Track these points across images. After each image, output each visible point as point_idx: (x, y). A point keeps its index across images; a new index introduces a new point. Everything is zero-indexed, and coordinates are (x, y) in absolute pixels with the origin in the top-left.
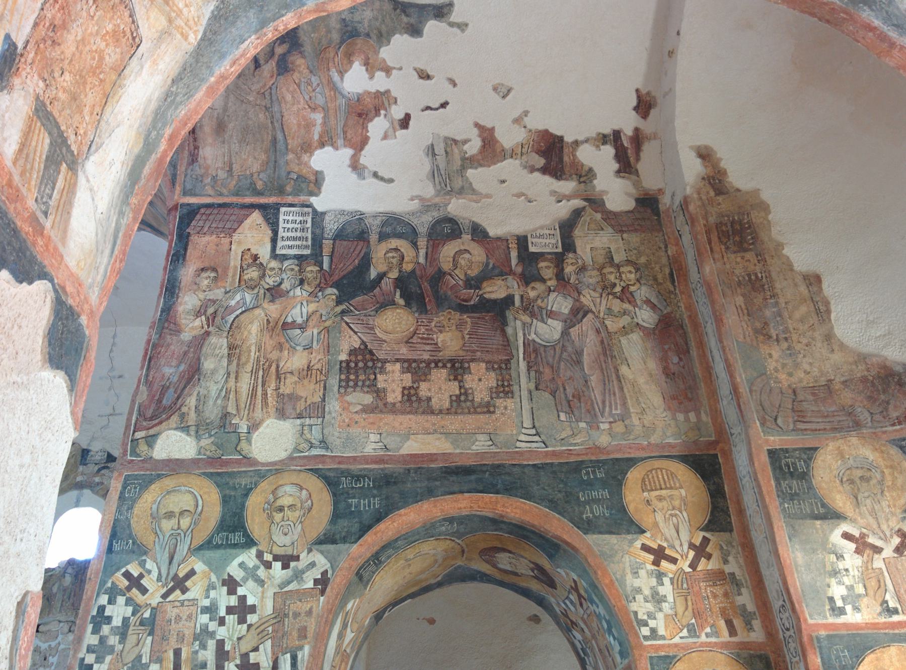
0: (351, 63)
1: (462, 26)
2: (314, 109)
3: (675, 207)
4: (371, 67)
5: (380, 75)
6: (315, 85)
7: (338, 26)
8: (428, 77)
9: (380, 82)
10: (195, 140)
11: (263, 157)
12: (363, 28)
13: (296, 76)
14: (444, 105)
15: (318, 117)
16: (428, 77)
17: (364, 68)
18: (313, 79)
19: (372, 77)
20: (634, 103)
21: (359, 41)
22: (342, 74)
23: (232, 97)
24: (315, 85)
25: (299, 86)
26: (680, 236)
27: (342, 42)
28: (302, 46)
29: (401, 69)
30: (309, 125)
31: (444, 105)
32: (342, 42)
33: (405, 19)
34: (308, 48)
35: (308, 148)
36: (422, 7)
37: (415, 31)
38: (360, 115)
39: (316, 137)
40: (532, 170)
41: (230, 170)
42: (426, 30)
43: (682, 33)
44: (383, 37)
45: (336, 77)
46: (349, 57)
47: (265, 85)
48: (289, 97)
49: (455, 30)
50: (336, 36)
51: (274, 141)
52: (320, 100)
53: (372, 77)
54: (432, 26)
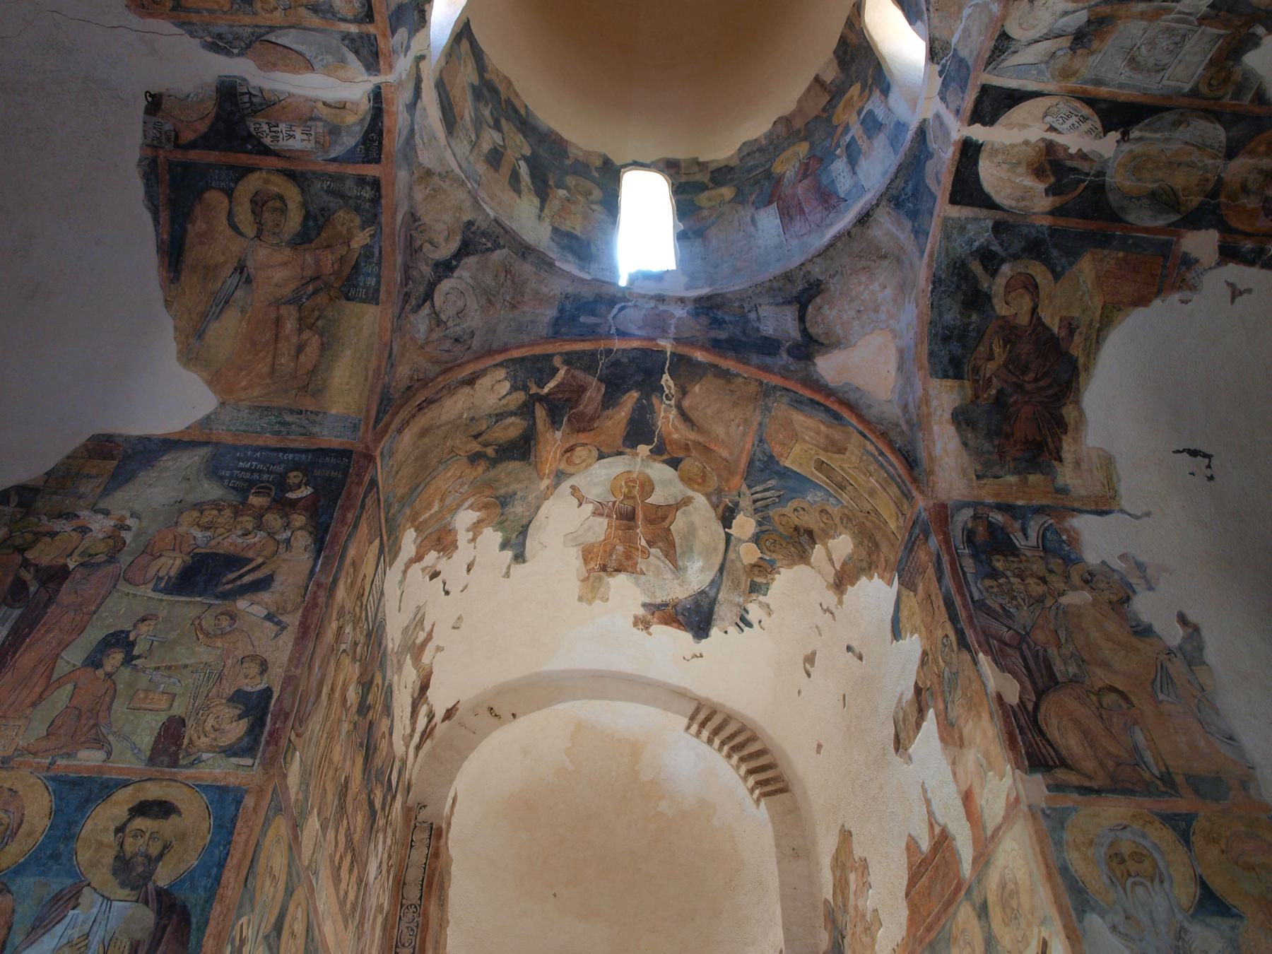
0: (479, 510)
1: (507, 575)
2: (442, 500)
3: (420, 818)
4: (476, 528)
5: (470, 535)
6: (461, 490)
7: (510, 491)
8: (469, 570)
9: (463, 537)
10: (414, 416)
11: (407, 490)
12: (509, 509)
13: (468, 471)
14: (447, 593)
15: (436, 508)
16: (469, 570)
17: (475, 520)
18: (466, 487)
19: (468, 530)
20: (450, 706)
21: (498, 510)
22: (471, 507)
23: (448, 427)
24: (461, 490)
25: (460, 477)
26: (412, 846)
27: (497, 498)
28: (494, 467)
29: (475, 548)
30: (429, 506)
31: (447, 593)
32: (497, 498)
33: (514, 536)
34: (492, 473)
35: (414, 518)
36: (523, 545)
37: (504, 546)
38: (439, 540)
39: (421, 519)
40: (412, 697)
41: (397, 473)
42: (505, 552)
43: (519, 721)
44: (500, 526)
45: (467, 504)
46: (486, 506)
47: (459, 449)
48: (449, 474)
49: (504, 570)
50: (502, 491)
51: (418, 486)
52: (448, 501)
53: (468, 530)
54: (509, 554)
